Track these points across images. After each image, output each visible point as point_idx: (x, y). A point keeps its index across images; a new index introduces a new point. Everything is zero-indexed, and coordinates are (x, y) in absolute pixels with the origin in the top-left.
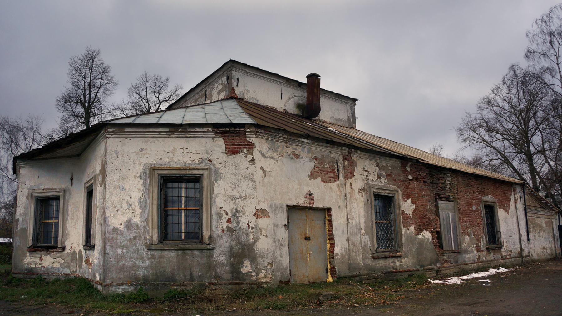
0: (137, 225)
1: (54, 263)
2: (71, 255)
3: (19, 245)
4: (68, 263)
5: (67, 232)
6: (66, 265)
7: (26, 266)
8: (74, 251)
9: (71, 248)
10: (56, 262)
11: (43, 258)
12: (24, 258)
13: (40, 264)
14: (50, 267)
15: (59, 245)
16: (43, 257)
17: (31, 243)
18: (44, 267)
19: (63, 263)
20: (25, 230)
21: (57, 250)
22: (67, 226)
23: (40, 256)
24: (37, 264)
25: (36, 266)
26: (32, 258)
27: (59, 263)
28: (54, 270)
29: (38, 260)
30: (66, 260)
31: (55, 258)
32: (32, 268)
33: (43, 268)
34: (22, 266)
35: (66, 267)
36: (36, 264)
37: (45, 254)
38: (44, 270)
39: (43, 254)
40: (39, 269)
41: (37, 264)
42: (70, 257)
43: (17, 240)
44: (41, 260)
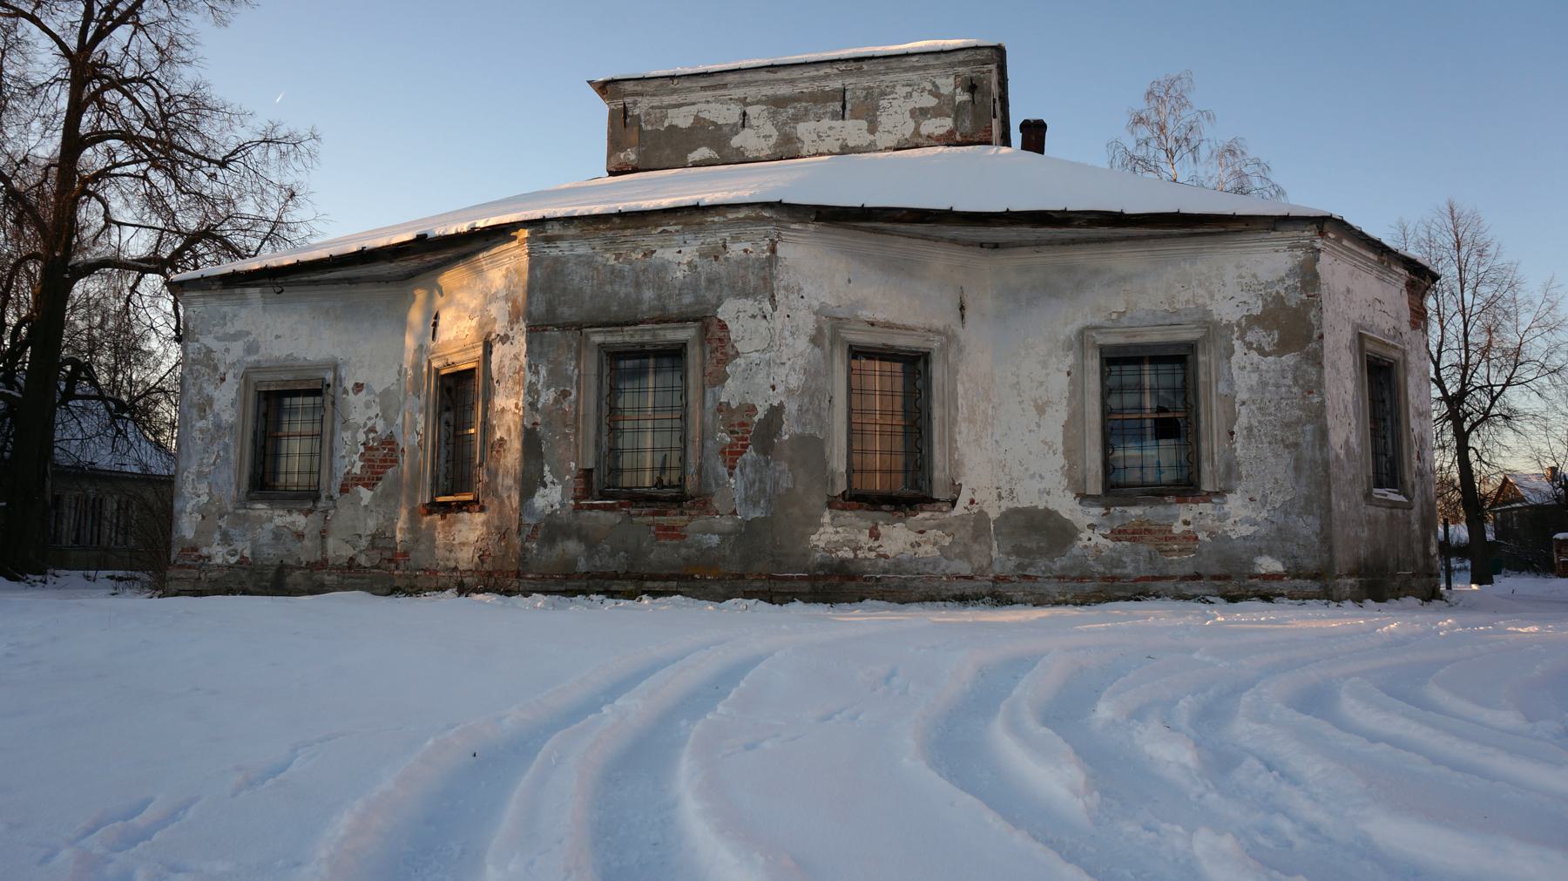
0: (1354, 449)
1: (919, 545)
2: (972, 523)
3: (788, 489)
4: (965, 545)
5: (956, 456)
6: (957, 551)
7: (818, 555)
8: (981, 512)
9: (972, 502)
10: (925, 542)
11: (882, 529)
12: (811, 530)
13: (870, 549)
14: (905, 557)
15: (938, 493)
16: (879, 528)
17: (841, 486)
18: (886, 557)
19: (947, 544)
20: (811, 447)
21: (939, 504)
22: (956, 441)
23: (870, 524)
24: (861, 548)
25: (856, 556)
26: (840, 529)
27: (934, 545)
28: (921, 566)
29: (864, 538)
30: (957, 536)
31: (922, 532)
32: (843, 561)
33: (881, 562)
34: (805, 555)
35: (958, 556)
36: (855, 550)
37: (888, 520)
38: (887, 566)
39: (882, 519)
40: (867, 563)
41: (861, 548)
42: (969, 529)
43: (782, 472)
44: (875, 535)
